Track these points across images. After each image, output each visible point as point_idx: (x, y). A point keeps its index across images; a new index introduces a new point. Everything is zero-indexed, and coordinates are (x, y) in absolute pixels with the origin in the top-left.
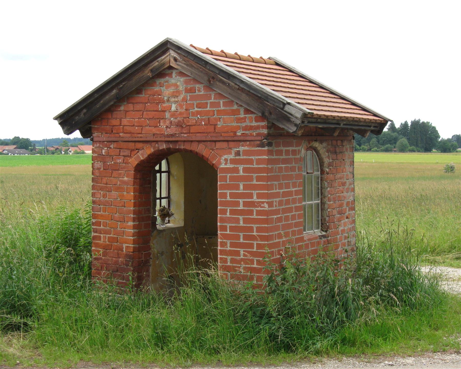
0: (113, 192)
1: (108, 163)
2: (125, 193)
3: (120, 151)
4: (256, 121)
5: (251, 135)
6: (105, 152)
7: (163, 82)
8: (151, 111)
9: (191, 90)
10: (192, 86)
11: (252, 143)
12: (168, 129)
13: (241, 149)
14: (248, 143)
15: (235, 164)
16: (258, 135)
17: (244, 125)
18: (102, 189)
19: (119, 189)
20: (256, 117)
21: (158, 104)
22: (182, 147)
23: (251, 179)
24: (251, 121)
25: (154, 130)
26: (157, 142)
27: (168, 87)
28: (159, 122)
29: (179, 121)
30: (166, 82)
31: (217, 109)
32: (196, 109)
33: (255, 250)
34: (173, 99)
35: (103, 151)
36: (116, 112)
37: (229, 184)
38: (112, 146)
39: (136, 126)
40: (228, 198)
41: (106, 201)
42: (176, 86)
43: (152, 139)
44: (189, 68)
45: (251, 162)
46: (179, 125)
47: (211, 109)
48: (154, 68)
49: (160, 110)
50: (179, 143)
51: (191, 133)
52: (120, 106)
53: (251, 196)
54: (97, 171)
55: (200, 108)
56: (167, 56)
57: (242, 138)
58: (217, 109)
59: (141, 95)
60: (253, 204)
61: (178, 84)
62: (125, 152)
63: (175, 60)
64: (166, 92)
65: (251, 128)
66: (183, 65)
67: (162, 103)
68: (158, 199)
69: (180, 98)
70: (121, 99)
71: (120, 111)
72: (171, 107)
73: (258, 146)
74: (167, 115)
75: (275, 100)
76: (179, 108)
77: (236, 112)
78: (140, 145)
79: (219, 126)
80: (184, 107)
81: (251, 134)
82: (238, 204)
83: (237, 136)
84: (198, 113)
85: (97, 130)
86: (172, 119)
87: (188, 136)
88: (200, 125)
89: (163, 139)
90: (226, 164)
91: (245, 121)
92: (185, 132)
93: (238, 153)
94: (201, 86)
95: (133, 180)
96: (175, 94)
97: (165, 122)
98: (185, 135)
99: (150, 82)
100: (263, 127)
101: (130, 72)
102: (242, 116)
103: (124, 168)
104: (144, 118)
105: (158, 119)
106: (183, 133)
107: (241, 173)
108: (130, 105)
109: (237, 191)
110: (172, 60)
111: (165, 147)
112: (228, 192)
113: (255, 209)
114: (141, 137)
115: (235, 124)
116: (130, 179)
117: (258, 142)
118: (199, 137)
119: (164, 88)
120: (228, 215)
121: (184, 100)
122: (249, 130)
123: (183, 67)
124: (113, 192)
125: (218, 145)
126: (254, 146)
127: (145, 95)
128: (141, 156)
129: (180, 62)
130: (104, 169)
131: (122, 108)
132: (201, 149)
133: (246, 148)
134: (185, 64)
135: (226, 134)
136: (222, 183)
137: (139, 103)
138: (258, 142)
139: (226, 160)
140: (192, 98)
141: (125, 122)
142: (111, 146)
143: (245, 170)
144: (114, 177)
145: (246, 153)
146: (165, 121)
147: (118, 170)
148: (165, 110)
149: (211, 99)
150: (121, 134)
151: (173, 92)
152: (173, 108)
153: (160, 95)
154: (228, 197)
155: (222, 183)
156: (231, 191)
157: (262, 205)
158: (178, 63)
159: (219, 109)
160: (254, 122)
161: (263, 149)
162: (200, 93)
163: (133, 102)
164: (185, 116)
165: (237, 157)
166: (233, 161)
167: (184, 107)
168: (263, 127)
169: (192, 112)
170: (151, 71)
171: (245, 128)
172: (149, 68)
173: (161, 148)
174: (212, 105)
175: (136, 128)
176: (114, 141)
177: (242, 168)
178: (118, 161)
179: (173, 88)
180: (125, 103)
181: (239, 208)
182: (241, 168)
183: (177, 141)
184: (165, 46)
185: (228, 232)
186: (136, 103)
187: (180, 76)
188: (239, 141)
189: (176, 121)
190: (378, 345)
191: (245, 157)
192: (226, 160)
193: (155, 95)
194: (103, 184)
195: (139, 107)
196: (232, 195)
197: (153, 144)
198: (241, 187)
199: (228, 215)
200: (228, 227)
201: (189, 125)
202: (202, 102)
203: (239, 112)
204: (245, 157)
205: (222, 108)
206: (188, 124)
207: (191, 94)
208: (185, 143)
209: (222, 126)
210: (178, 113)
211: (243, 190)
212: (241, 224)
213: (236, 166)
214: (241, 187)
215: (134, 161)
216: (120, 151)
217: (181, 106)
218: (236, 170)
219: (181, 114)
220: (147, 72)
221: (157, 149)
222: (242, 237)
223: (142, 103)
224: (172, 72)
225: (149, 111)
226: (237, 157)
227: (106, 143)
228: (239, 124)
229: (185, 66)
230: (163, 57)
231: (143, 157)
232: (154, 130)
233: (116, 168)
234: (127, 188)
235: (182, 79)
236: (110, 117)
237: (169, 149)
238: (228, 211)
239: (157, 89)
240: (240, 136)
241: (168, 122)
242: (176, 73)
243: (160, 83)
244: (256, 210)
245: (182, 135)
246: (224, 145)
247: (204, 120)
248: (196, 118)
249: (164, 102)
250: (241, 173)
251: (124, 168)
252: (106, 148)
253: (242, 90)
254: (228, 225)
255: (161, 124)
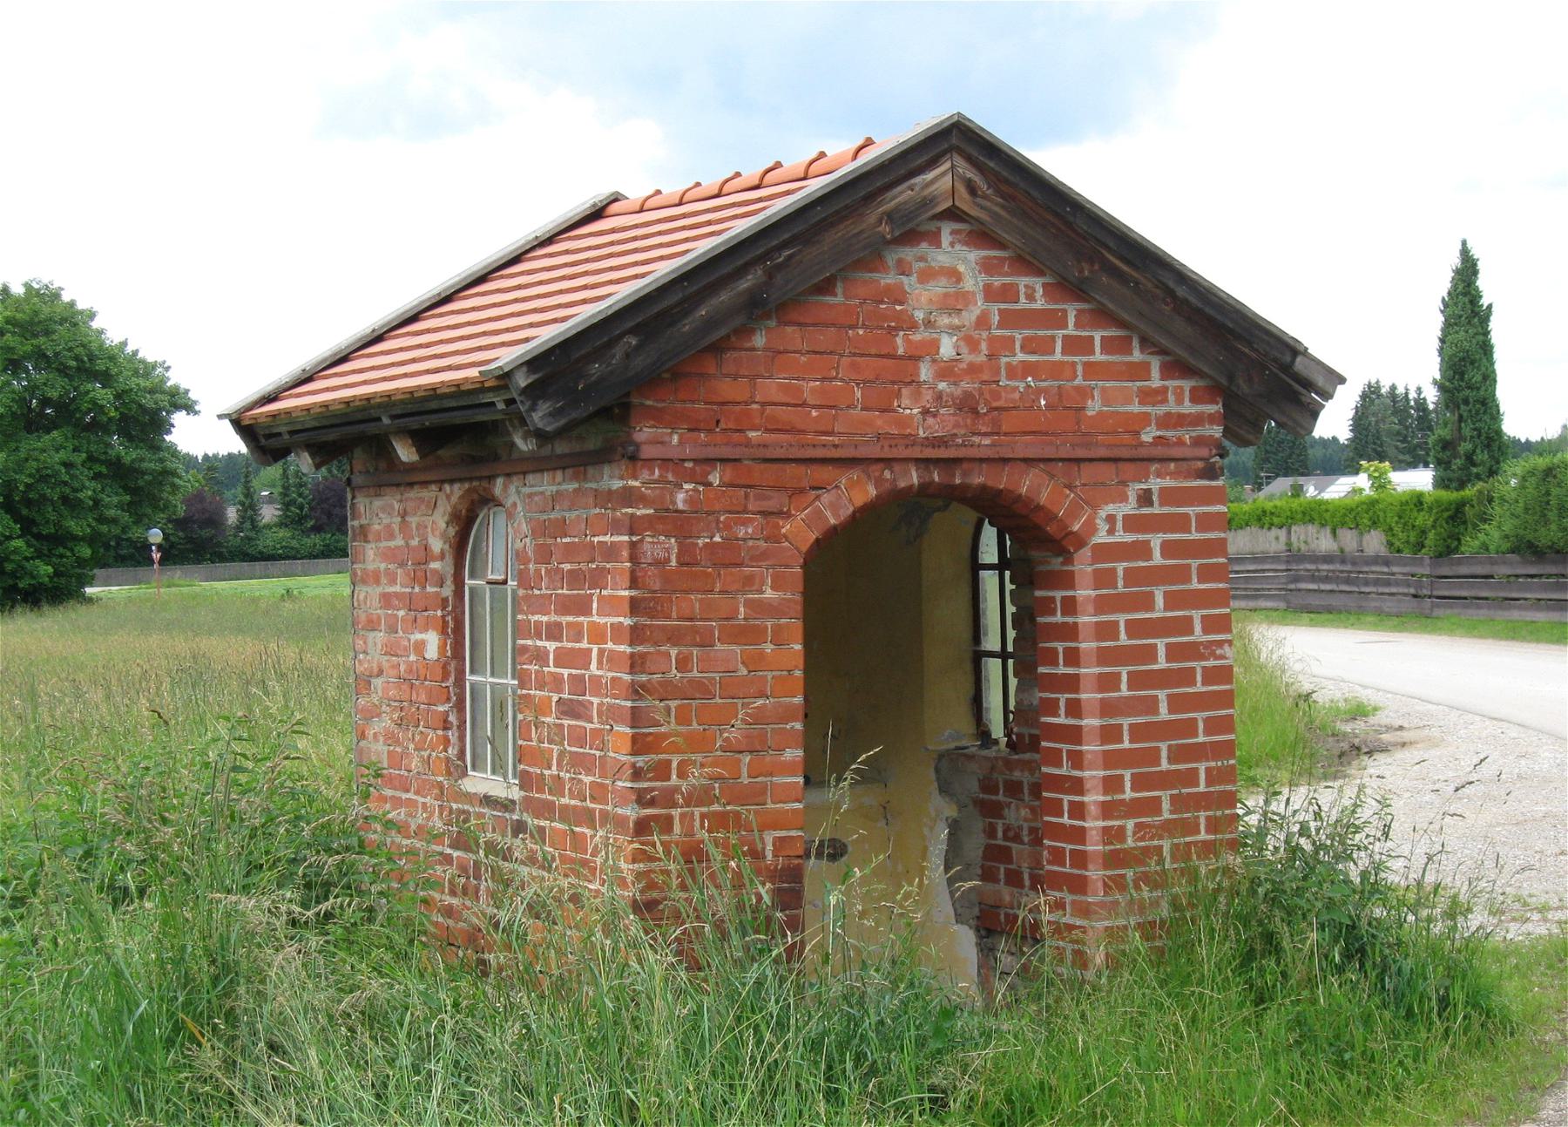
0: (719, 646)
1: (700, 542)
2: (769, 648)
3: (746, 496)
4: (1194, 400)
5: (1180, 442)
6: (685, 501)
7: (909, 258)
8: (870, 355)
9: (1008, 293)
10: (1007, 280)
11: (1184, 465)
12: (930, 421)
13: (1155, 484)
14: (1172, 465)
15: (1138, 531)
16: (1198, 442)
17: (1161, 410)
18: (674, 637)
19: (746, 634)
20: (1193, 390)
21: (893, 331)
22: (977, 480)
23: (1182, 574)
24: (1181, 397)
25: (879, 422)
26: (887, 462)
27: (927, 276)
28: (898, 395)
29: (967, 395)
30: (922, 259)
31: (1085, 359)
32: (1021, 357)
33: (1202, 788)
34: (945, 320)
35: (680, 497)
36: (736, 354)
37: (1124, 594)
38: (715, 478)
39: (814, 407)
40: (1123, 639)
41: (691, 681)
42: (956, 276)
43: (874, 451)
44: (1015, 221)
45: (1181, 523)
46: (967, 405)
47: (1066, 358)
48: (897, 209)
49: (901, 351)
50: (965, 465)
51: (1006, 434)
52: (752, 331)
53: (1185, 626)
54: (652, 571)
55: (1033, 353)
56: (943, 174)
57: (1159, 451)
58: (1085, 359)
59: (829, 299)
60: (1192, 651)
61: (961, 268)
62: (769, 498)
63: (972, 189)
64: (921, 297)
65: (1180, 421)
66: (997, 209)
67: (909, 329)
68: (1011, 656)
69: (970, 316)
70: (757, 308)
71: (754, 349)
72: (935, 345)
73: (1201, 477)
74: (925, 372)
75: (1272, 341)
76: (964, 350)
77: (1141, 371)
78: (825, 473)
79: (1090, 413)
80: (984, 346)
81: (1179, 438)
82: (1149, 654)
83: (1142, 444)
84: (1028, 369)
85: (657, 417)
86: (942, 386)
87: (993, 445)
88: (1032, 407)
89: (916, 453)
90: (1111, 531)
91: (1164, 401)
92: (984, 429)
93: (1145, 498)
94: (1038, 283)
95: (798, 597)
96: (954, 303)
97: (917, 396)
98: (987, 441)
99: (871, 256)
100: (1212, 419)
101: (820, 213)
102: (1156, 382)
103: (764, 555)
104: (842, 380)
105: (894, 383)
106: (979, 434)
107: (1157, 559)
108: (789, 329)
109: (1147, 616)
110: (962, 190)
111: (915, 480)
112: (1121, 618)
113: (1198, 665)
114: (836, 446)
115: (1135, 408)
116: (789, 596)
117: (1200, 464)
118: (1024, 447)
119: (914, 278)
120: (1124, 691)
121: (982, 322)
122: (1175, 427)
123: (996, 213)
124: (719, 646)
125: (1088, 472)
126: (1189, 475)
127: (846, 297)
128: (828, 514)
129: (985, 197)
130: (681, 564)
131: (759, 340)
132: (1028, 484)
133: (1168, 482)
134: (1003, 207)
135: (1110, 439)
136: (1104, 592)
137: (827, 325)
138: (1200, 464)
139: (1111, 519)
140: (1008, 319)
141: (770, 388)
142: (711, 478)
143: (1167, 549)
144: (721, 592)
145: (1168, 496)
146: (919, 393)
147: (740, 565)
148: (918, 353)
149: (1065, 326)
150: (752, 434)
151: (946, 295)
152: (947, 348)
153: (901, 303)
154: (1123, 635)
155: (1104, 592)
156: (1130, 617)
157: (1218, 652)
158: (979, 200)
159: (1092, 358)
160: (1187, 402)
161: (1214, 483)
162: (1034, 306)
163: (802, 320)
164: (985, 378)
165: (1146, 511)
166: (1132, 523)
167: (984, 346)
168: (1212, 419)
169: (1008, 364)
170: (889, 217)
171: (1167, 421)
172: (880, 204)
173: (902, 484)
174: (1072, 345)
175: (814, 413)
176: (722, 460)
177: (1158, 542)
178: (741, 532)
179: (943, 281)
180: (772, 323)
181: (1155, 667)
182: (1156, 541)
183: (957, 461)
184: (958, 139)
185: (1126, 745)
186: (814, 325)
187: (966, 244)
188: (1142, 461)
189: (958, 392)
190: (1261, 999)
191: (1166, 510)
192: (1111, 519)
193: (882, 302)
194: (680, 619)
195: (825, 338)
196: (1134, 628)
197: (875, 469)
198: (1159, 601)
199: (1124, 691)
200: (1126, 728)
201: (996, 409)
202: (1040, 333)
203: (1149, 371)
204: (1166, 510)
205: (1098, 356)
206: (995, 404)
207: (1003, 306)
208: (1121, 465)
209: (1100, 413)
210: (963, 366)
211: (1166, 609)
212: (1164, 713)
213: (1141, 537)
214: (1159, 601)
215: (800, 530)
216: (746, 496)
217: (973, 345)
218: (1143, 550)
219: (973, 369)
220: (872, 218)
221: (887, 485)
222: (1164, 754)
223: (834, 325)
224: (939, 229)
225: (862, 355)
226: (1146, 511)
227: (689, 465)
228: (1148, 409)
229: (1003, 213)
230: (929, 176)
231: (835, 515)
232: (881, 422)
233: (728, 557)
234: (777, 630)
235: (974, 255)
236: (712, 371)
237: (925, 489)
238: (1124, 678)
239: (888, 279)
240: (1151, 444)
241: (927, 396)
242: (953, 232)
243: (900, 262)
244: (1204, 668)
245: (976, 439)
246: (1107, 472)
247: (1045, 391)
248: (1022, 386)
249: (913, 326)
250: (1157, 559)
251: (764, 555)
252: (686, 486)
253: (1180, 306)
254: (1126, 722)
255: (905, 402)
